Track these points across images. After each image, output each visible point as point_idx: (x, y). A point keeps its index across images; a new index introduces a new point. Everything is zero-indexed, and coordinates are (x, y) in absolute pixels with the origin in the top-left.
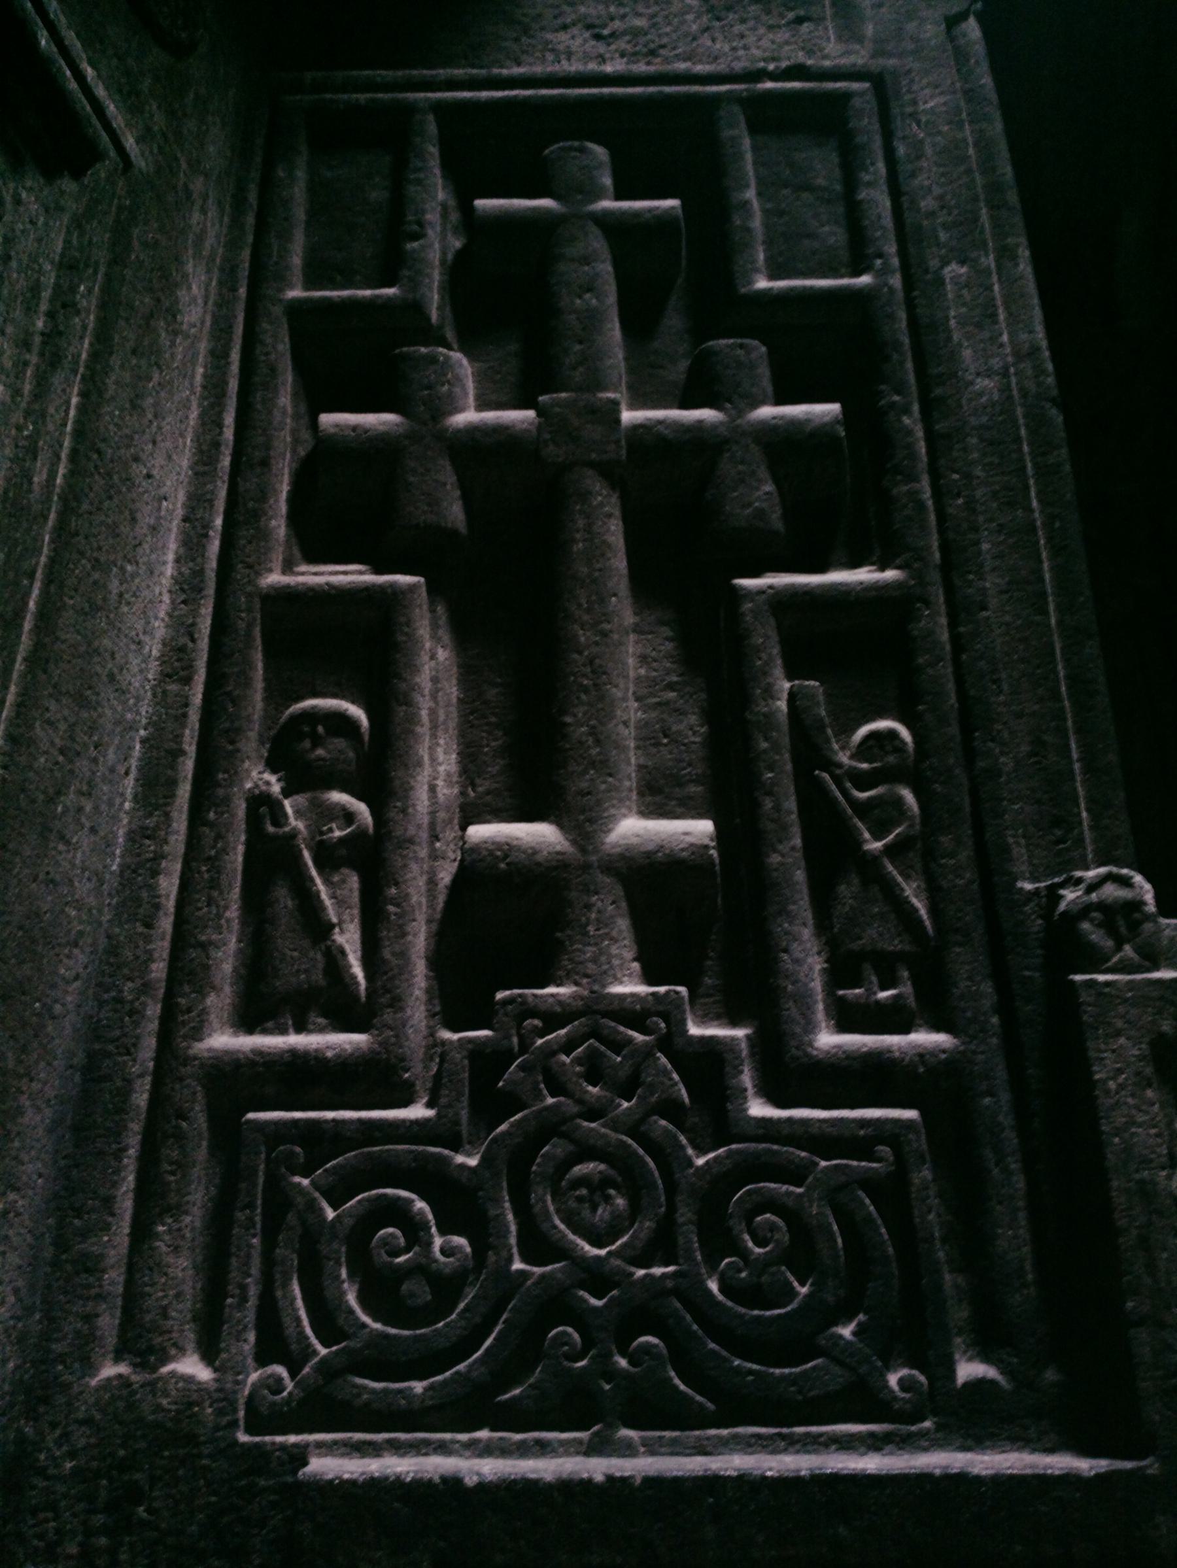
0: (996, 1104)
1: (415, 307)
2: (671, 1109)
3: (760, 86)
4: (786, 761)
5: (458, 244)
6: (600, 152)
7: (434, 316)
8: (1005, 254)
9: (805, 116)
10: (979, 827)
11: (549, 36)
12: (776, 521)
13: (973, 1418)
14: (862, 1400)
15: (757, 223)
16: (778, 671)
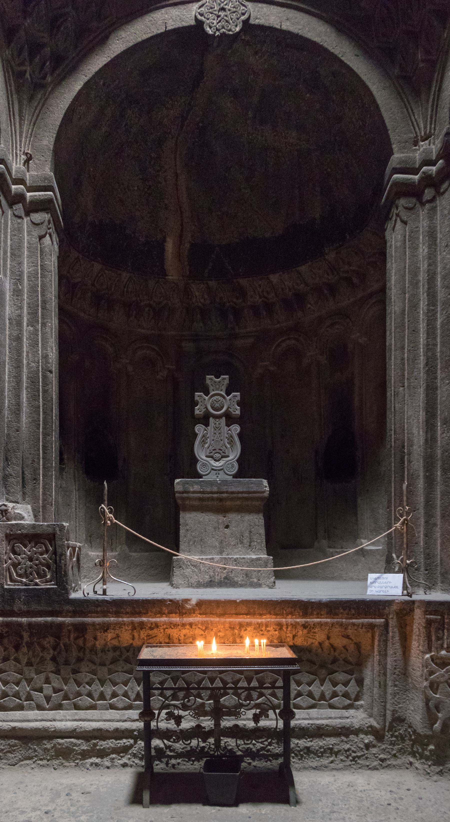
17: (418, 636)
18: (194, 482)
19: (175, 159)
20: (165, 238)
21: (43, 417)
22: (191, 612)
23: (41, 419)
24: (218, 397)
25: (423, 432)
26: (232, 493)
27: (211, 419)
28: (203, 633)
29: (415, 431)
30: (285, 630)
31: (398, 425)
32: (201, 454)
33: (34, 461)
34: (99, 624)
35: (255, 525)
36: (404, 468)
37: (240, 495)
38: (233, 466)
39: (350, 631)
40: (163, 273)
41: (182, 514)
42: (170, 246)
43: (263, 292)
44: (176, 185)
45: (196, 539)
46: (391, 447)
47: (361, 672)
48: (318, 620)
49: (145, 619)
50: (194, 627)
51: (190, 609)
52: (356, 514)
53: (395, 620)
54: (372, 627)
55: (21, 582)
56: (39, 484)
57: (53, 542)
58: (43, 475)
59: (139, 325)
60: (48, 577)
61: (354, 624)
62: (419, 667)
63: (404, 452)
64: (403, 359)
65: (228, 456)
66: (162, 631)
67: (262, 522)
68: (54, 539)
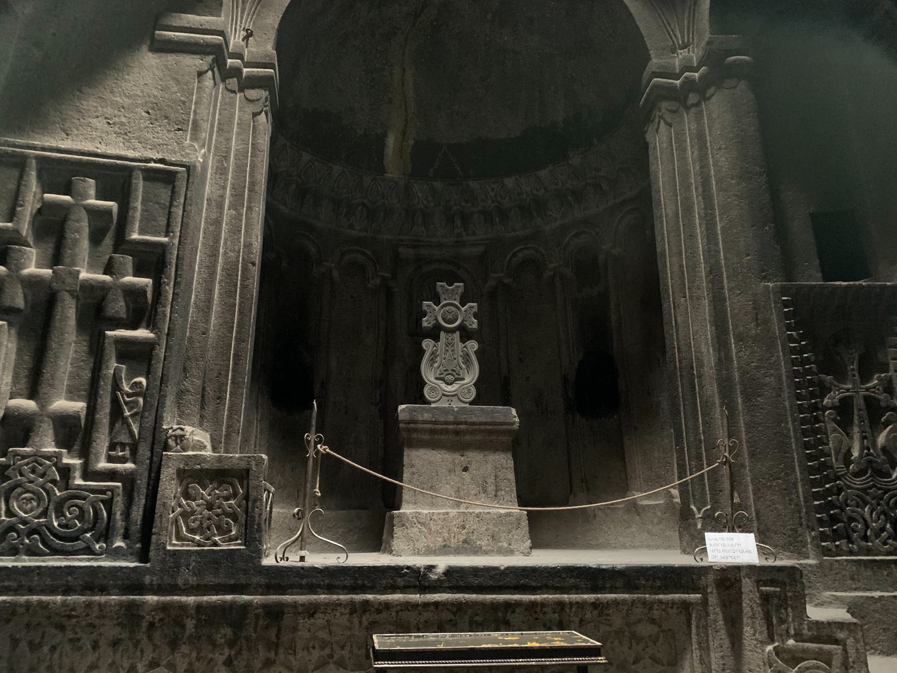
0: (142, 483)
1: (17, 231)
2: (54, 482)
3: (149, 165)
4: (109, 388)
5: (39, 206)
6: (92, 182)
7: (24, 234)
8: (250, 209)
9: (164, 177)
10: (157, 410)
11: (90, 120)
12: (123, 314)
13: (117, 554)
14: (89, 551)
15: (138, 215)
16: (114, 359)
17: (751, 618)
26: (473, 424)
28: (452, 617)
34: (303, 605)
37: (482, 427)
39: (656, 613)
46: (675, 368)
49: (370, 597)
50: (440, 608)
53: (715, 595)
55: (193, 540)
60: (233, 533)
61: (660, 602)
62: (758, 666)
65: (464, 379)
66: (394, 614)
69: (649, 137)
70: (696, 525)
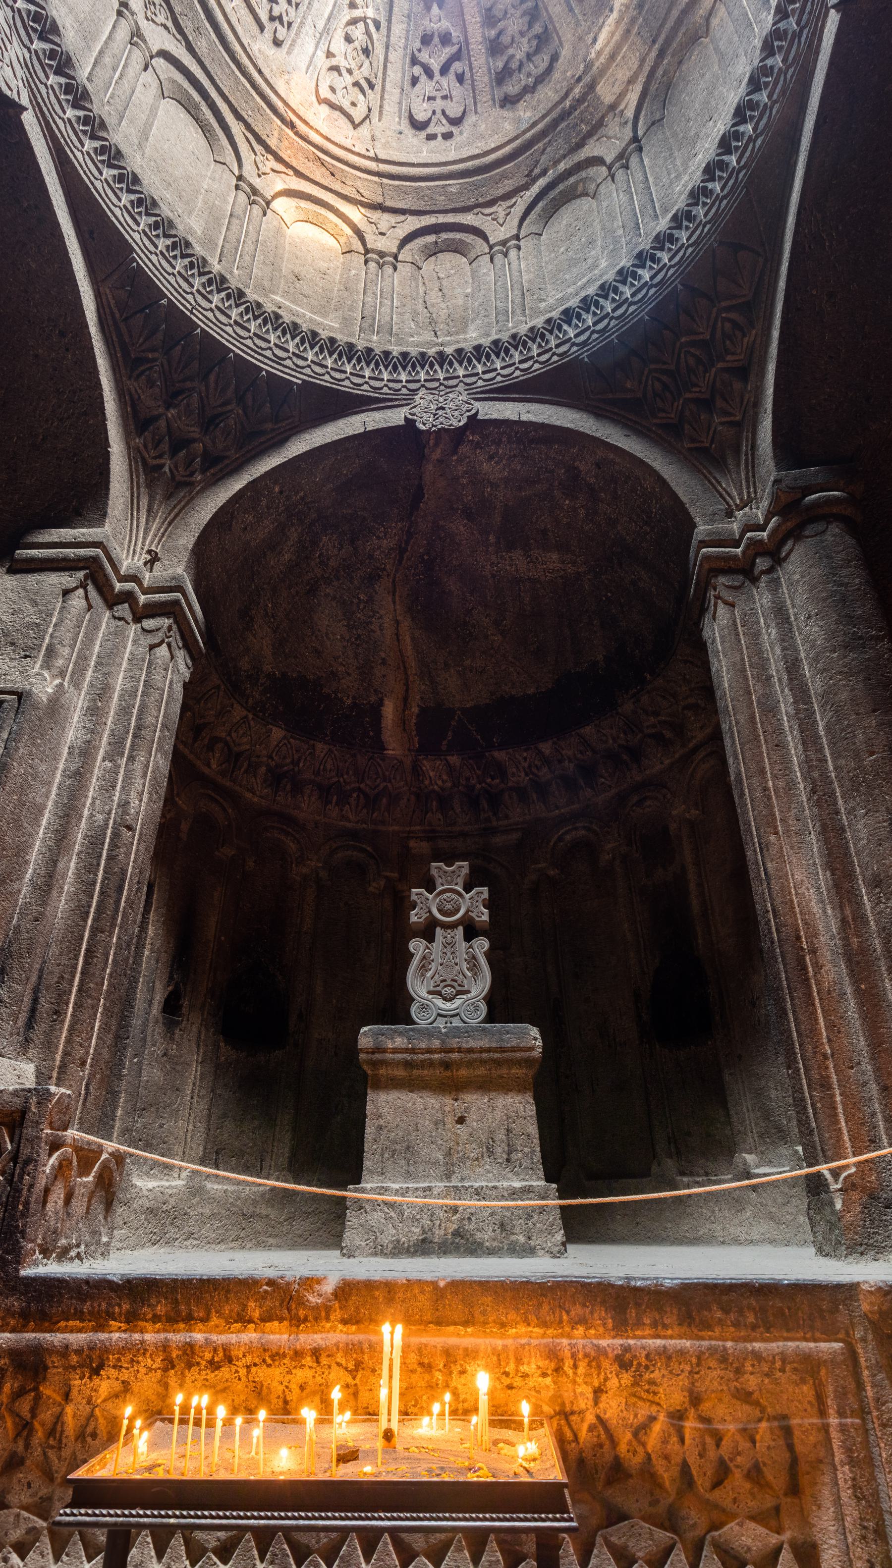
18: (395, 1031)
19: (394, 603)
20: (382, 700)
21: (98, 901)
22: (321, 1314)
23: (94, 904)
24: (451, 895)
25: (833, 908)
26: (470, 1051)
27: (438, 929)
29: (815, 907)
30: (570, 1372)
31: (778, 901)
32: (418, 987)
33: (63, 977)
35: (518, 1117)
36: (807, 979)
37: (485, 1056)
38: (477, 1008)
39: (752, 1382)
40: (381, 746)
41: (371, 1095)
42: (389, 710)
43: (530, 767)
44: (397, 635)
45: (398, 1147)
47: (805, 1522)
48: (659, 1342)
49: (198, 1337)
51: (316, 1308)
52: (724, 1104)
54: (809, 1366)
56: (63, 1021)
57: (17, 1132)
58: (75, 1004)
59: (343, 816)
61: (757, 1356)
63: (802, 949)
64: (766, 789)
65: (468, 992)
67: (531, 1109)
68: (21, 1124)
69: (706, 634)
70: (832, 1204)
